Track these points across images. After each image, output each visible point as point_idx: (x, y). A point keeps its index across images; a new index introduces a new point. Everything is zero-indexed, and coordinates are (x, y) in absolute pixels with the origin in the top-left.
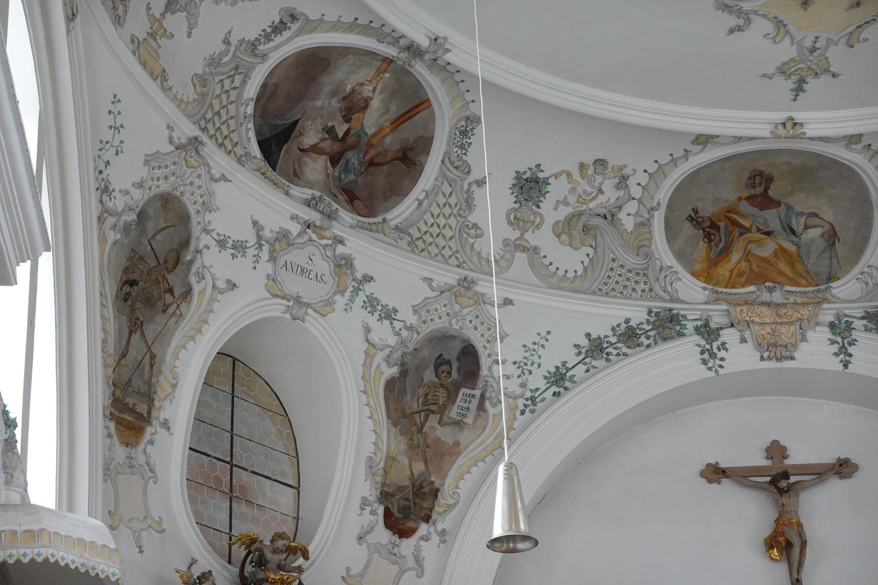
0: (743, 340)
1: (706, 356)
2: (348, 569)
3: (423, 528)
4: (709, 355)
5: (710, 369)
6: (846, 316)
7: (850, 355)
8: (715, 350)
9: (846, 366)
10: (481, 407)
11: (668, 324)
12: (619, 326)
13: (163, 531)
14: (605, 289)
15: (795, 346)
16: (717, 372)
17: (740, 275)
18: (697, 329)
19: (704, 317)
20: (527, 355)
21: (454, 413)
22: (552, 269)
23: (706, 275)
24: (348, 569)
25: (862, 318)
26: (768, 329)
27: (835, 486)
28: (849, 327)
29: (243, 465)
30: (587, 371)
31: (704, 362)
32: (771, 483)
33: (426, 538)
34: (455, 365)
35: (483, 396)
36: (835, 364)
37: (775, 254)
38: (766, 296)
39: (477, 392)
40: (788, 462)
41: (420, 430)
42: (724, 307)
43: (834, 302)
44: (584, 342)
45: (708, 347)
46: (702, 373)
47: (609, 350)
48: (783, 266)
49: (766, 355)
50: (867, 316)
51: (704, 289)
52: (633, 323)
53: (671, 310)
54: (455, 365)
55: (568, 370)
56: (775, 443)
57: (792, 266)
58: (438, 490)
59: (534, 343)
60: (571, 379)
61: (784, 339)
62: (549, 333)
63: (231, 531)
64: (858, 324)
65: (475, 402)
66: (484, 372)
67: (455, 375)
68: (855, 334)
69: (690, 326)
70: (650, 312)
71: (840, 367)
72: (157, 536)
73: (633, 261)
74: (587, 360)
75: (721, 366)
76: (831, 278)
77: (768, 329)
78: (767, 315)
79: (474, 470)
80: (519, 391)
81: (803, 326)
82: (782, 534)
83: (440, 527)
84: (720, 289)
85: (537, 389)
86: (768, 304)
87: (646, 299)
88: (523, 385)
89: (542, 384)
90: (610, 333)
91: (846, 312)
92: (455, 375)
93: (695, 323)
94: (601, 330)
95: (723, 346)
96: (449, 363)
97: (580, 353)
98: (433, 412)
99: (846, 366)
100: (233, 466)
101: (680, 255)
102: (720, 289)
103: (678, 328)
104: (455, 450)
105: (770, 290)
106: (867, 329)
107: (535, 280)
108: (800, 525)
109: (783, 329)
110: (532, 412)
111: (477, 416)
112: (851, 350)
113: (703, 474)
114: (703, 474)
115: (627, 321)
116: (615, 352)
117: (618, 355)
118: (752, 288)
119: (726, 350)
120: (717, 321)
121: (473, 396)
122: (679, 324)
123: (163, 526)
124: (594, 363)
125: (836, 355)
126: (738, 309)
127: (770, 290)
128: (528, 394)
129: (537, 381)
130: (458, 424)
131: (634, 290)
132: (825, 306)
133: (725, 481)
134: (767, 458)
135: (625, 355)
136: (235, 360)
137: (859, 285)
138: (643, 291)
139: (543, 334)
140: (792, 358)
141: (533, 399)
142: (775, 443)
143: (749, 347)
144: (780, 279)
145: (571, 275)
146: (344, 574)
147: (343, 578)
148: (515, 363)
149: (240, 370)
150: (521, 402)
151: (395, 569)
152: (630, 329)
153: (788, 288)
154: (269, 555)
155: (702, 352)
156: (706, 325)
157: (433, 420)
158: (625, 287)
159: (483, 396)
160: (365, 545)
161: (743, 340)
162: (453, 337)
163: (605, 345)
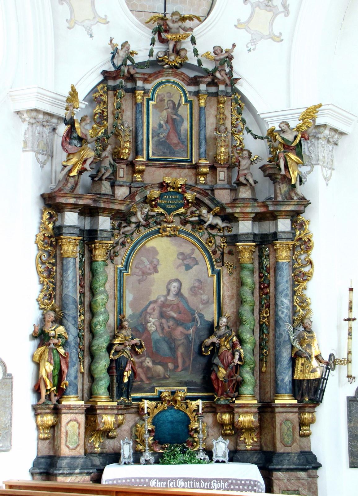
2: (239, 20)
13: (108, 22)
24: (239, 20)
63: (165, 11)
72: (104, 26)
123: (108, 20)
146: (236, 24)
147: (235, 26)
151: (270, 14)
160: (249, 5)
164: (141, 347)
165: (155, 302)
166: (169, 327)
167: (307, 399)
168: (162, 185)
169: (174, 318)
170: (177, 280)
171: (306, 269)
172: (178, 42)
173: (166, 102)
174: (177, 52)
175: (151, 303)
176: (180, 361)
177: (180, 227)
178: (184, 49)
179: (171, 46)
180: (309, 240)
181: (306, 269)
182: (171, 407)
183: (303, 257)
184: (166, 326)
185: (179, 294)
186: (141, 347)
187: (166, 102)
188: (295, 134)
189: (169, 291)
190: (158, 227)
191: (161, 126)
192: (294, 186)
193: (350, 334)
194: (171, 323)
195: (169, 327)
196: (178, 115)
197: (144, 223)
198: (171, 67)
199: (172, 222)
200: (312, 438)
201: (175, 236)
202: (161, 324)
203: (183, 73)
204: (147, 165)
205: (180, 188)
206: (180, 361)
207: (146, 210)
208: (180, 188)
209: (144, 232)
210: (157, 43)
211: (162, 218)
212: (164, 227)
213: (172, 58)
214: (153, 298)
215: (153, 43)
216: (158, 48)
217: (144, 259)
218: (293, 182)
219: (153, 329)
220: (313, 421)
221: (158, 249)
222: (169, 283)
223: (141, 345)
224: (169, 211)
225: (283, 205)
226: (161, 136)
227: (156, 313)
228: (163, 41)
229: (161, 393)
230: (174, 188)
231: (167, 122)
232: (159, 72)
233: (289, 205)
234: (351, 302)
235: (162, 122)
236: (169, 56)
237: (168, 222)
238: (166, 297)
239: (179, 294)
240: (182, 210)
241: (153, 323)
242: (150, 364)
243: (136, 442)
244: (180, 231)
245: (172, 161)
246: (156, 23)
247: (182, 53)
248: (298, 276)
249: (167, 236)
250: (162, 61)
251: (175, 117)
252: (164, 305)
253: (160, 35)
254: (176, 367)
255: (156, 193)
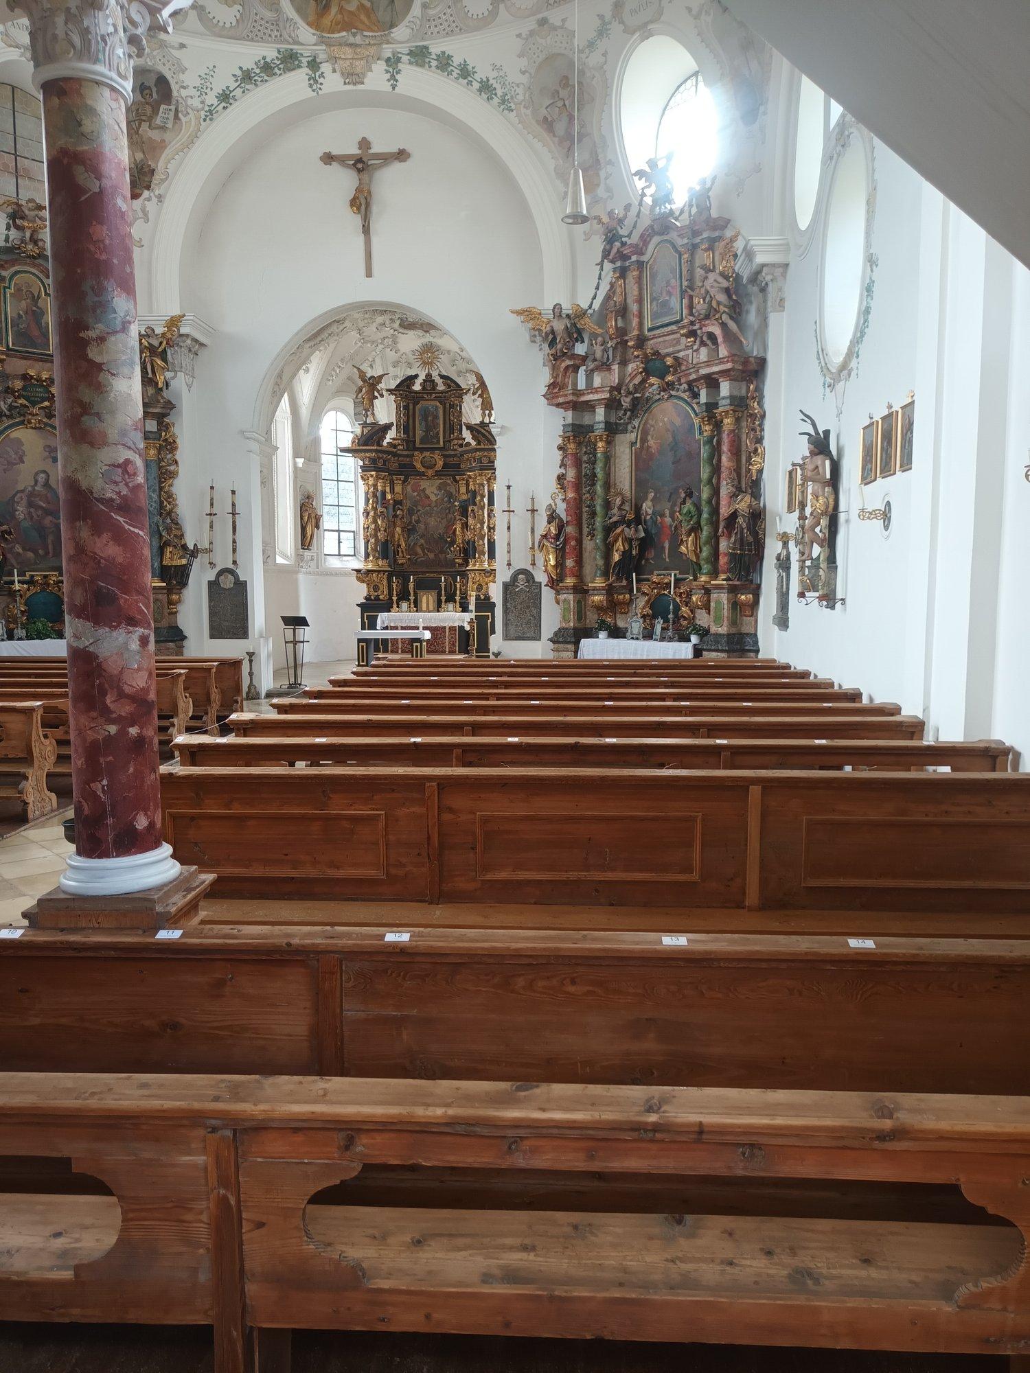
0: (334, 71)
1: (312, 82)
3: (146, 193)
4: (314, 81)
5: (313, 91)
6: (399, 53)
7: (397, 81)
8: (317, 78)
9: (394, 89)
10: (176, 117)
11: (290, 60)
12: (259, 61)
14: (250, 35)
15: (364, 75)
16: (317, 93)
17: (337, 24)
18: (308, 62)
19: (313, 54)
20: (202, 82)
21: (158, 121)
22: (215, 21)
23: (316, 24)
25: (408, 54)
26: (348, 63)
27: (397, 167)
28: (399, 60)
29: (26, 155)
30: (243, 92)
31: (311, 86)
32: (354, 165)
33: (149, 199)
34: (154, 90)
35: (177, 111)
36: (387, 87)
37: (358, 7)
38: (352, 40)
39: (173, 107)
40: (372, 151)
41: (137, 133)
42: (324, 47)
43: (391, 43)
44: (239, 73)
45: (313, 75)
46: (310, 93)
47: (256, 78)
48: (363, 17)
49: (347, 80)
50: (411, 53)
51: (314, 34)
52: (268, 60)
53: (292, 50)
54: (154, 90)
55: (231, 92)
56: (364, 138)
57: (369, 17)
58: (154, 170)
59: (206, 74)
60: (234, 98)
61: (358, 70)
62: (214, 67)
63: (18, 196)
64: (405, 58)
65: (172, 114)
66: (175, 93)
67: (155, 96)
68: (401, 66)
69: (305, 61)
70: (279, 52)
71: (390, 89)
73: (268, 15)
74: (243, 85)
75: (320, 89)
76: (392, 26)
77: (348, 63)
78: (348, 52)
79: (176, 157)
80: (200, 106)
81: (369, 61)
82: (358, 198)
83: (157, 192)
84: (324, 35)
85: (212, 105)
86: (351, 45)
87: (275, 42)
88: (203, 102)
89: (215, 102)
90: (255, 67)
91: (398, 50)
92: (155, 96)
93: (307, 59)
94: (249, 65)
95: (322, 75)
96: (149, 88)
97: (237, 81)
98: (144, 121)
99: (394, 89)
100: (16, 155)
101: (299, 10)
102: (324, 35)
103: (297, 63)
104: (162, 145)
105: (354, 35)
106: (410, 63)
107: (202, 29)
108: (369, 193)
109: (357, 63)
110: (211, 119)
111: (175, 123)
112: (397, 77)
113: (321, 159)
114: (321, 159)
115: (264, 58)
116: (260, 79)
117: (262, 81)
118: (344, 33)
119: (324, 77)
120: (322, 56)
121: (170, 110)
122: (297, 58)
124: (247, 87)
125: (388, 80)
126: (332, 49)
127: (354, 35)
128: (207, 108)
129: (211, 99)
130: (163, 128)
131: (270, 36)
132: (385, 46)
133: (334, 163)
134: (360, 148)
135: (266, 81)
136: (13, 88)
137: (409, 31)
138: (276, 36)
139: (211, 68)
140: (363, 83)
141: (210, 111)
142: (364, 138)
143: (337, 76)
144: (361, 26)
145: (228, 25)
148: (195, 88)
149: (18, 94)
150: (203, 113)
152: (266, 63)
153: (365, 33)
154: (27, 212)
155: (309, 80)
156: (314, 60)
157: (145, 126)
158: (265, 34)
159: (177, 111)
161: (334, 71)
162: (149, 71)
163: (253, 75)
164: (10, 533)
165: (22, 491)
166: (38, 516)
167: (174, 582)
168: (25, 377)
169: (41, 507)
170: (44, 472)
171: (172, 468)
172: (34, 231)
173: (24, 291)
174: (35, 241)
175: (18, 492)
176: (50, 547)
177: (45, 420)
178: (42, 240)
179: (28, 234)
180: (174, 441)
181: (172, 468)
182: (43, 590)
183: (169, 457)
184: (35, 516)
185: (46, 484)
186: (10, 533)
187: (24, 291)
188: (160, 340)
189: (36, 482)
190: (22, 418)
191: (20, 316)
192: (161, 389)
193: (211, 527)
194: (40, 512)
195: (38, 516)
196: (38, 307)
197: (8, 413)
198: (29, 257)
199: (37, 414)
200: (179, 616)
201: (40, 428)
202: (30, 513)
203: (41, 265)
204: (7, 355)
205: (44, 381)
206: (50, 547)
207: (9, 401)
208: (44, 381)
209: (7, 423)
210: (12, 229)
211: (26, 409)
212: (28, 420)
213: (30, 247)
214: (20, 487)
215: (8, 228)
216: (13, 234)
217: (8, 449)
218: (160, 385)
219: (22, 517)
220: (179, 601)
221: (23, 440)
222: (37, 474)
223: (11, 532)
224: (34, 404)
225: (152, 407)
226: (21, 327)
227: (24, 502)
228: (18, 228)
229: (32, 577)
230: (38, 381)
231: (26, 313)
232: (16, 260)
233: (156, 407)
234: (212, 499)
235: (21, 312)
236: (26, 244)
237: (33, 415)
238: (33, 487)
239: (46, 484)
240: (46, 404)
241: (21, 511)
242: (20, 550)
243: (8, 622)
244: (46, 424)
245: (34, 353)
246: (10, 207)
247: (40, 244)
248: (165, 473)
249: (32, 428)
250: (19, 248)
251: (34, 308)
252: (32, 494)
253: (14, 222)
254: (47, 553)
255: (18, 384)
